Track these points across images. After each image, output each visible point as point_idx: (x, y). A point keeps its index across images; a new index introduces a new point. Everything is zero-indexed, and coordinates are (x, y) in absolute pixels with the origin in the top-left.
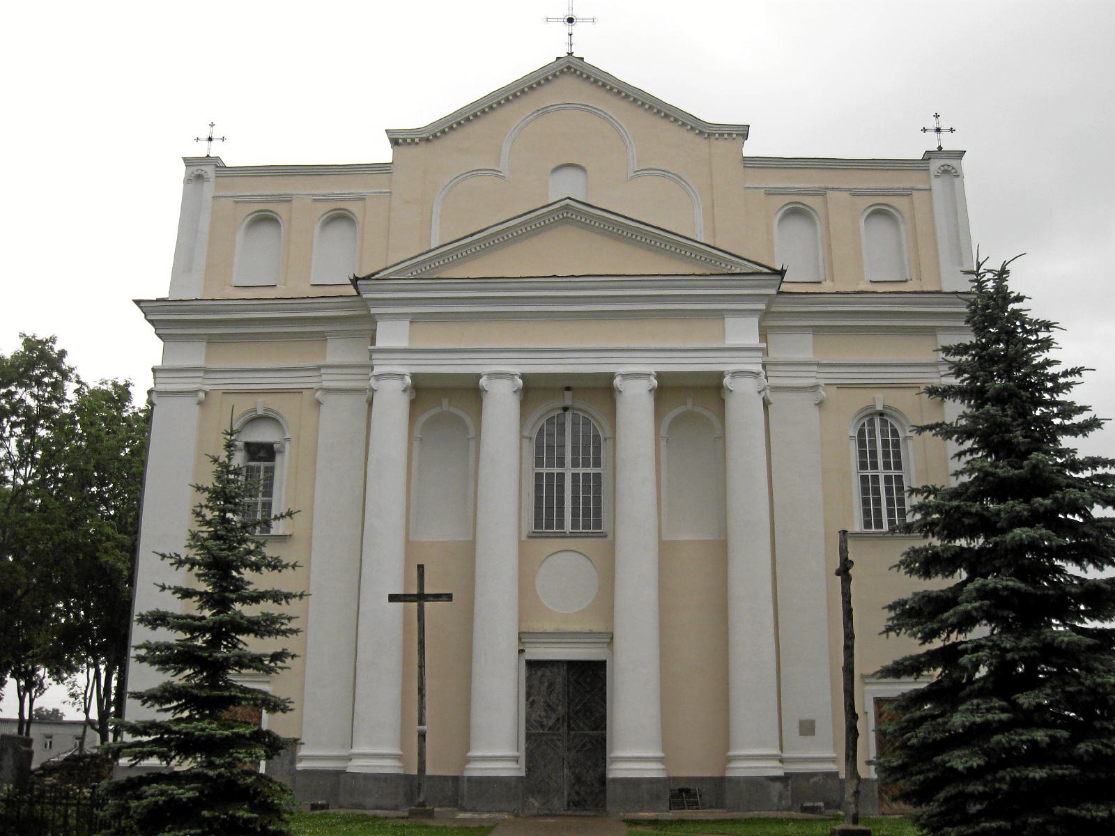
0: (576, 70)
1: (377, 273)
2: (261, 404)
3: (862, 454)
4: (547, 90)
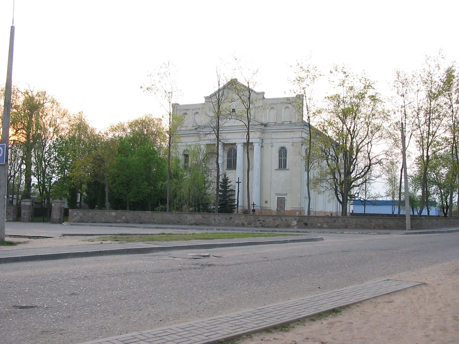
3: (280, 155)
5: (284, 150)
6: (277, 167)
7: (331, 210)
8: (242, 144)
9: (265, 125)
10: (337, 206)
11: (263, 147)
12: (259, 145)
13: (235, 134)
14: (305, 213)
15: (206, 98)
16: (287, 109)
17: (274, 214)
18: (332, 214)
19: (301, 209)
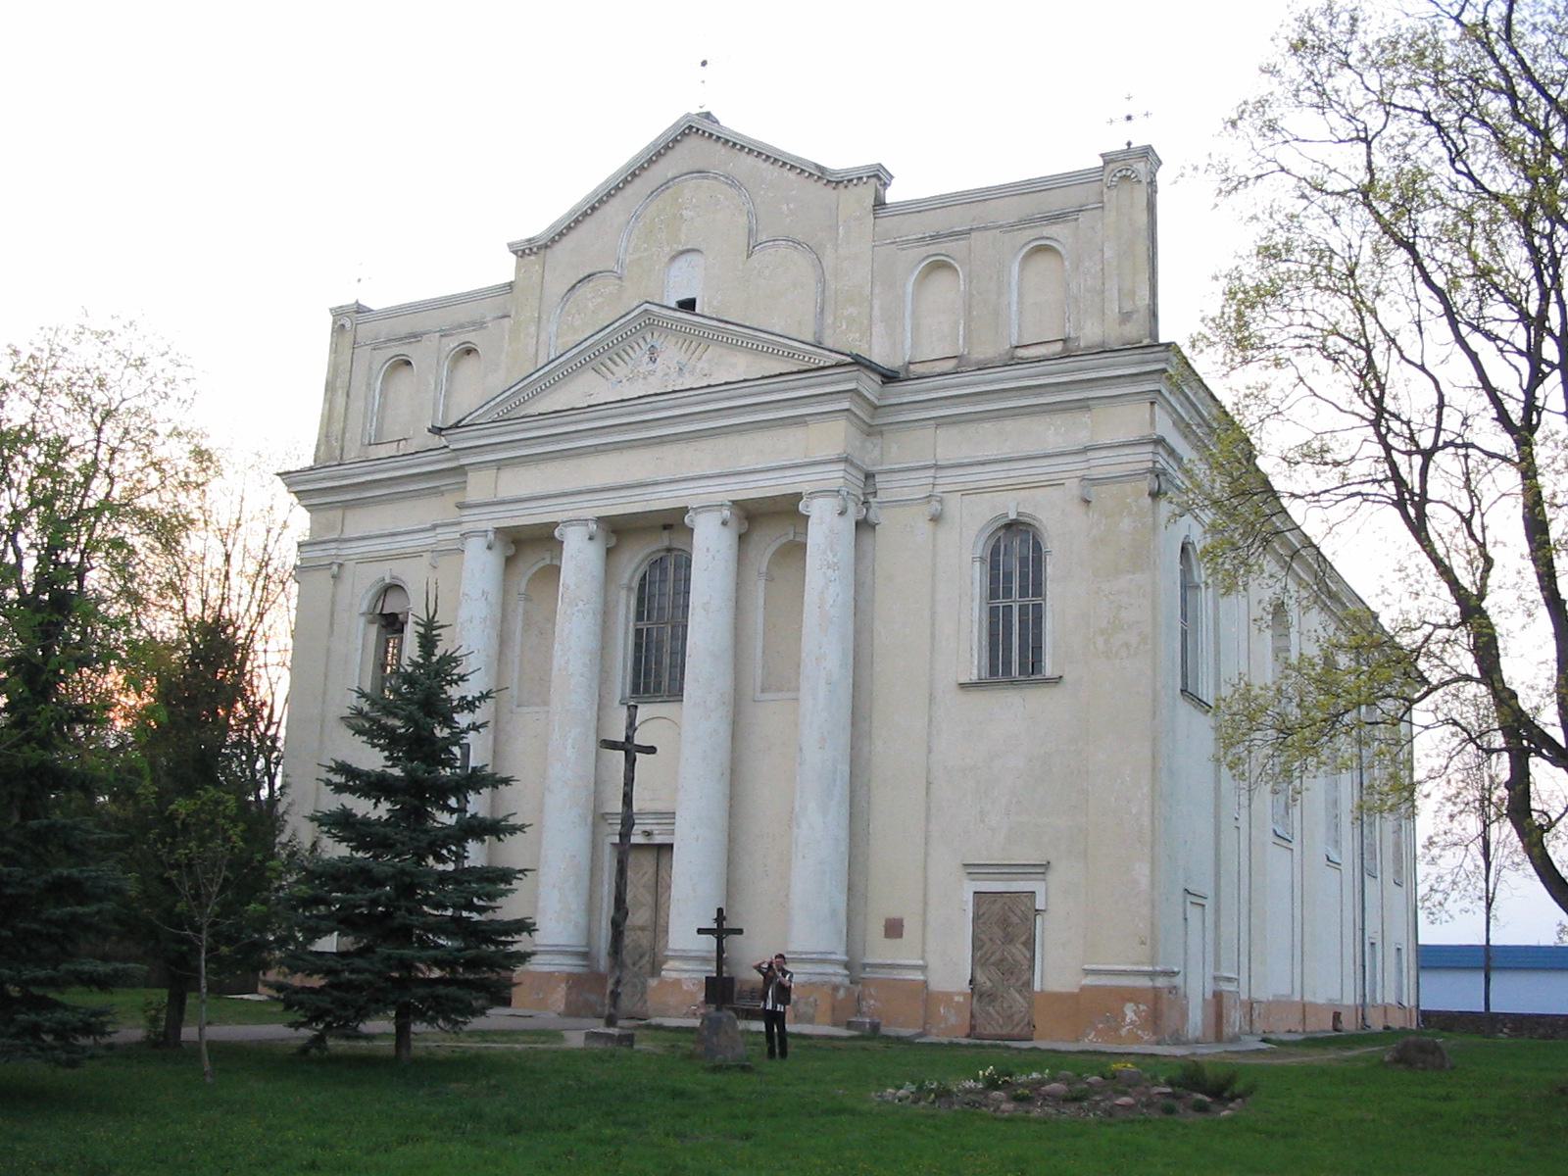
0: (698, 130)
1: (464, 419)
2: (386, 572)
3: (994, 580)
4: (663, 163)
5: (1024, 542)
6: (972, 665)
7: (1335, 995)
8: (726, 513)
9: (889, 377)
10: (1364, 967)
11: (873, 527)
12: (841, 514)
13: (682, 446)
14: (1184, 1015)
15: (526, 251)
16: (1044, 262)
17: (949, 1026)
18: (1337, 1016)
19: (1161, 982)
